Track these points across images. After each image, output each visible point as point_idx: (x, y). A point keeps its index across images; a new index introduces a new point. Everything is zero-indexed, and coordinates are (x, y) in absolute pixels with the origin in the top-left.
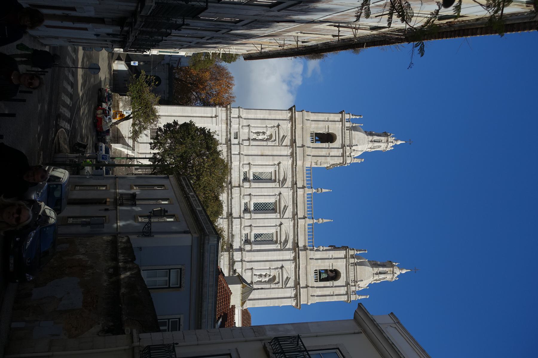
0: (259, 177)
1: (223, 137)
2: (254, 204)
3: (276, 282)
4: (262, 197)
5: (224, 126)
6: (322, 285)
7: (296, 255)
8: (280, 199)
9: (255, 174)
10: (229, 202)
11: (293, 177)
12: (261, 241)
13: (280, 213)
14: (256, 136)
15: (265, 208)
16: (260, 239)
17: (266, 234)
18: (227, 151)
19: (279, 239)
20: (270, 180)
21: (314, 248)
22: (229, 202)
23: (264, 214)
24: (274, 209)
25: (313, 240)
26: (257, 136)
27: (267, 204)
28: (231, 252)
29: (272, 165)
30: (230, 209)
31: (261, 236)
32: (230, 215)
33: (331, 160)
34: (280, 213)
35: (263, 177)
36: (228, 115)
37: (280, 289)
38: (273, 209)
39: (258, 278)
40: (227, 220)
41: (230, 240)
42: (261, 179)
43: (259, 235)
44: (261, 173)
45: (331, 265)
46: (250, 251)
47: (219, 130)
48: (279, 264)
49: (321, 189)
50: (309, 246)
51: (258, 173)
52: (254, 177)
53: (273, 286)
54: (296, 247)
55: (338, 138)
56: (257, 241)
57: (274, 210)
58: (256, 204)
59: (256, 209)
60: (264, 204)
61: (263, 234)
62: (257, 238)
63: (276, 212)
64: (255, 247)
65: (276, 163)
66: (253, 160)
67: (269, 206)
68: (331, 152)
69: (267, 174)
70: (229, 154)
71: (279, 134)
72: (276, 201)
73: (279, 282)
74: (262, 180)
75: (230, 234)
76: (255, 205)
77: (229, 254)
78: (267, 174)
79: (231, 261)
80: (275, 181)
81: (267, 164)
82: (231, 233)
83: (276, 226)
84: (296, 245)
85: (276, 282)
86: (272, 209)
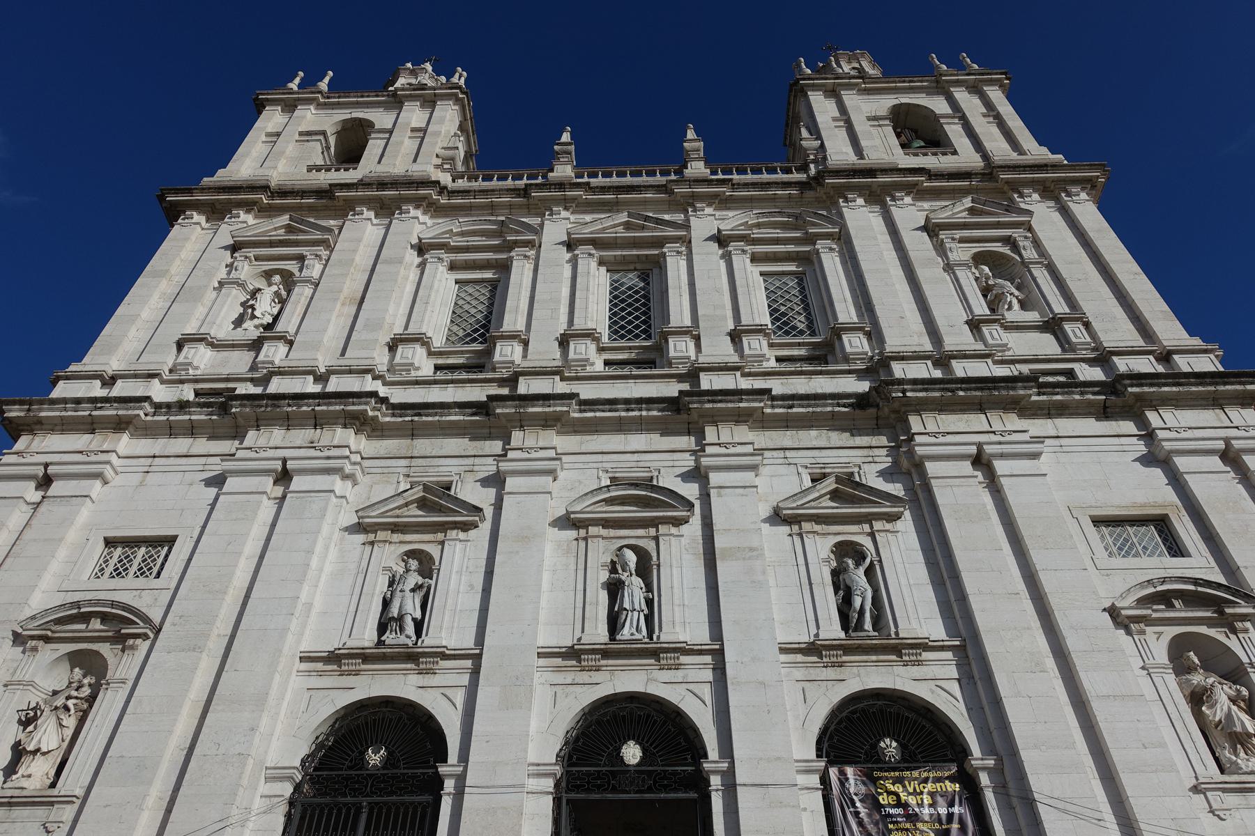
0: (478, 321)
1: (194, 451)
2: (615, 339)
3: (1006, 250)
4: (577, 301)
5: (124, 443)
6: (966, 141)
7: (859, 189)
8: (595, 243)
9: (454, 338)
10: (598, 414)
11: (492, 208)
12: (809, 314)
13: (660, 243)
14: (256, 322)
15: (637, 301)
16: (802, 318)
17: (768, 297)
18: (289, 422)
19: (791, 248)
20: (497, 291)
21: (813, 161)
22: (598, 414)
23: (670, 291)
24: (642, 274)
25: (775, 164)
26: (253, 317)
27: (616, 297)
28: (908, 394)
29: (422, 273)
30: (644, 413)
31: (784, 314)
32: (678, 411)
33: (442, 121)
34: (660, 243)
35: (477, 310)
36: (64, 413)
37: (1041, 235)
38: (644, 277)
39: (1010, 308)
40: (710, 434)
41: (829, 409)
42: (486, 317)
43: (777, 319)
44: (456, 317)
45: (876, 123)
46: (875, 334)
47: (146, 469)
48: (918, 246)
49: (558, 144)
50: (804, 168)
51: (455, 328)
52: (474, 340)
53: (1030, 253)
54: (820, 192)
55: (355, 115)
56: (809, 327)
57: (652, 270)
58: (616, 332)
59: (644, 331)
60: (616, 305)
61: (769, 306)
62: (794, 328)
63: (659, 264)
64: (846, 311)
65: (413, 258)
66: (376, 326)
67: (630, 288)
68: (409, 124)
69: (468, 298)
70: (305, 408)
71: (271, 244)
72: (601, 263)
73: (1009, 241)
74: (491, 313)
75: (795, 410)
76: (622, 337)
77: (921, 407)
78: (468, 298)
79: (961, 393)
80: (504, 268)
81: (410, 288)
82: (791, 407)
83: (727, 257)
84: (809, 194)
85: (1006, 250)
86: (643, 280)
